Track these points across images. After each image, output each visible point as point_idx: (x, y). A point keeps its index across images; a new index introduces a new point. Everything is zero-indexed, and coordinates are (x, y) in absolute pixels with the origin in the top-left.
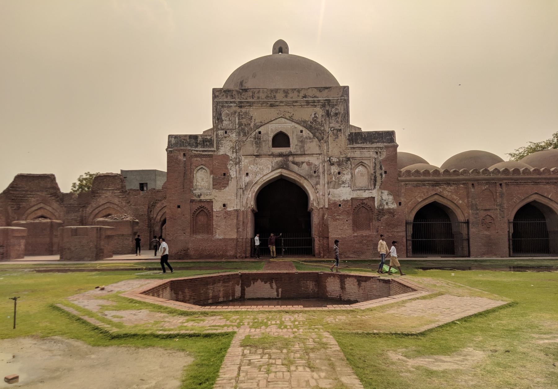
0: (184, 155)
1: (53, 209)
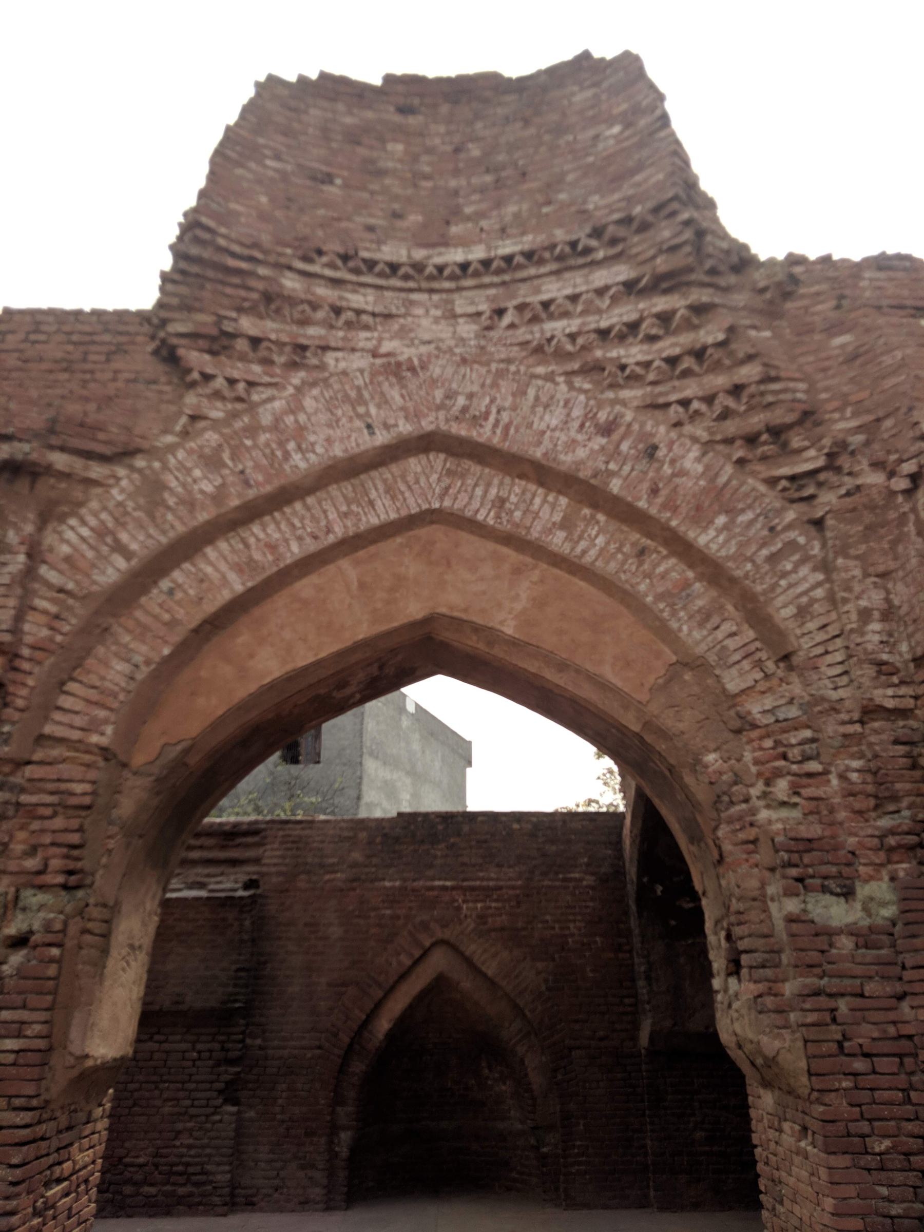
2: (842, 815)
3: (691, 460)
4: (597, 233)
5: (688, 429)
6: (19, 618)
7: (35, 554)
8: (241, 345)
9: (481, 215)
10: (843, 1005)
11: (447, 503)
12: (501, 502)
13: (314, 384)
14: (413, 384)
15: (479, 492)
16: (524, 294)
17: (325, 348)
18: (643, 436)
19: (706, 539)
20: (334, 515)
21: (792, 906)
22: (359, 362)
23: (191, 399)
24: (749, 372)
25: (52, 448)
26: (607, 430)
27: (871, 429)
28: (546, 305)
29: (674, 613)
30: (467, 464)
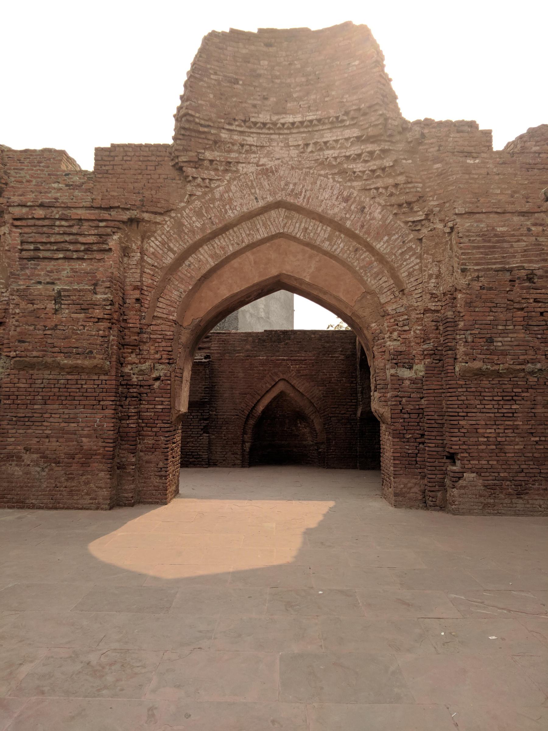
2: (413, 344)
3: (377, 214)
4: (347, 113)
5: (377, 200)
6: (141, 276)
7: (143, 253)
8: (206, 163)
9: (301, 98)
10: (404, 400)
11: (286, 230)
12: (306, 229)
13: (234, 179)
14: (273, 178)
15: (297, 225)
16: (316, 137)
17: (238, 163)
18: (361, 202)
19: (379, 246)
21: (393, 371)
22: (252, 169)
23: (189, 188)
24: (401, 179)
25: (143, 212)
26: (346, 200)
27: (441, 206)
28: (326, 143)
29: (366, 274)
30: (293, 213)
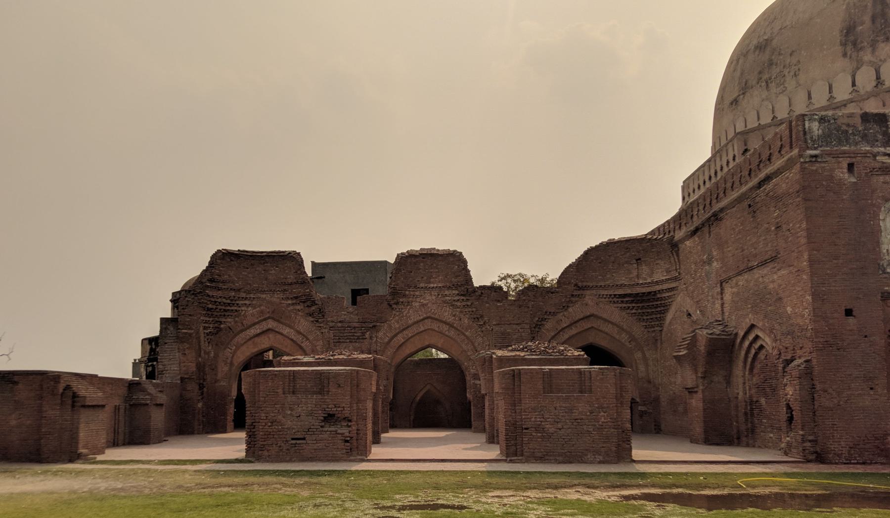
0: (851, 167)
1: (299, 333)
3: (466, 321)
20: (414, 330)
22: (417, 304)
26: (454, 316)
